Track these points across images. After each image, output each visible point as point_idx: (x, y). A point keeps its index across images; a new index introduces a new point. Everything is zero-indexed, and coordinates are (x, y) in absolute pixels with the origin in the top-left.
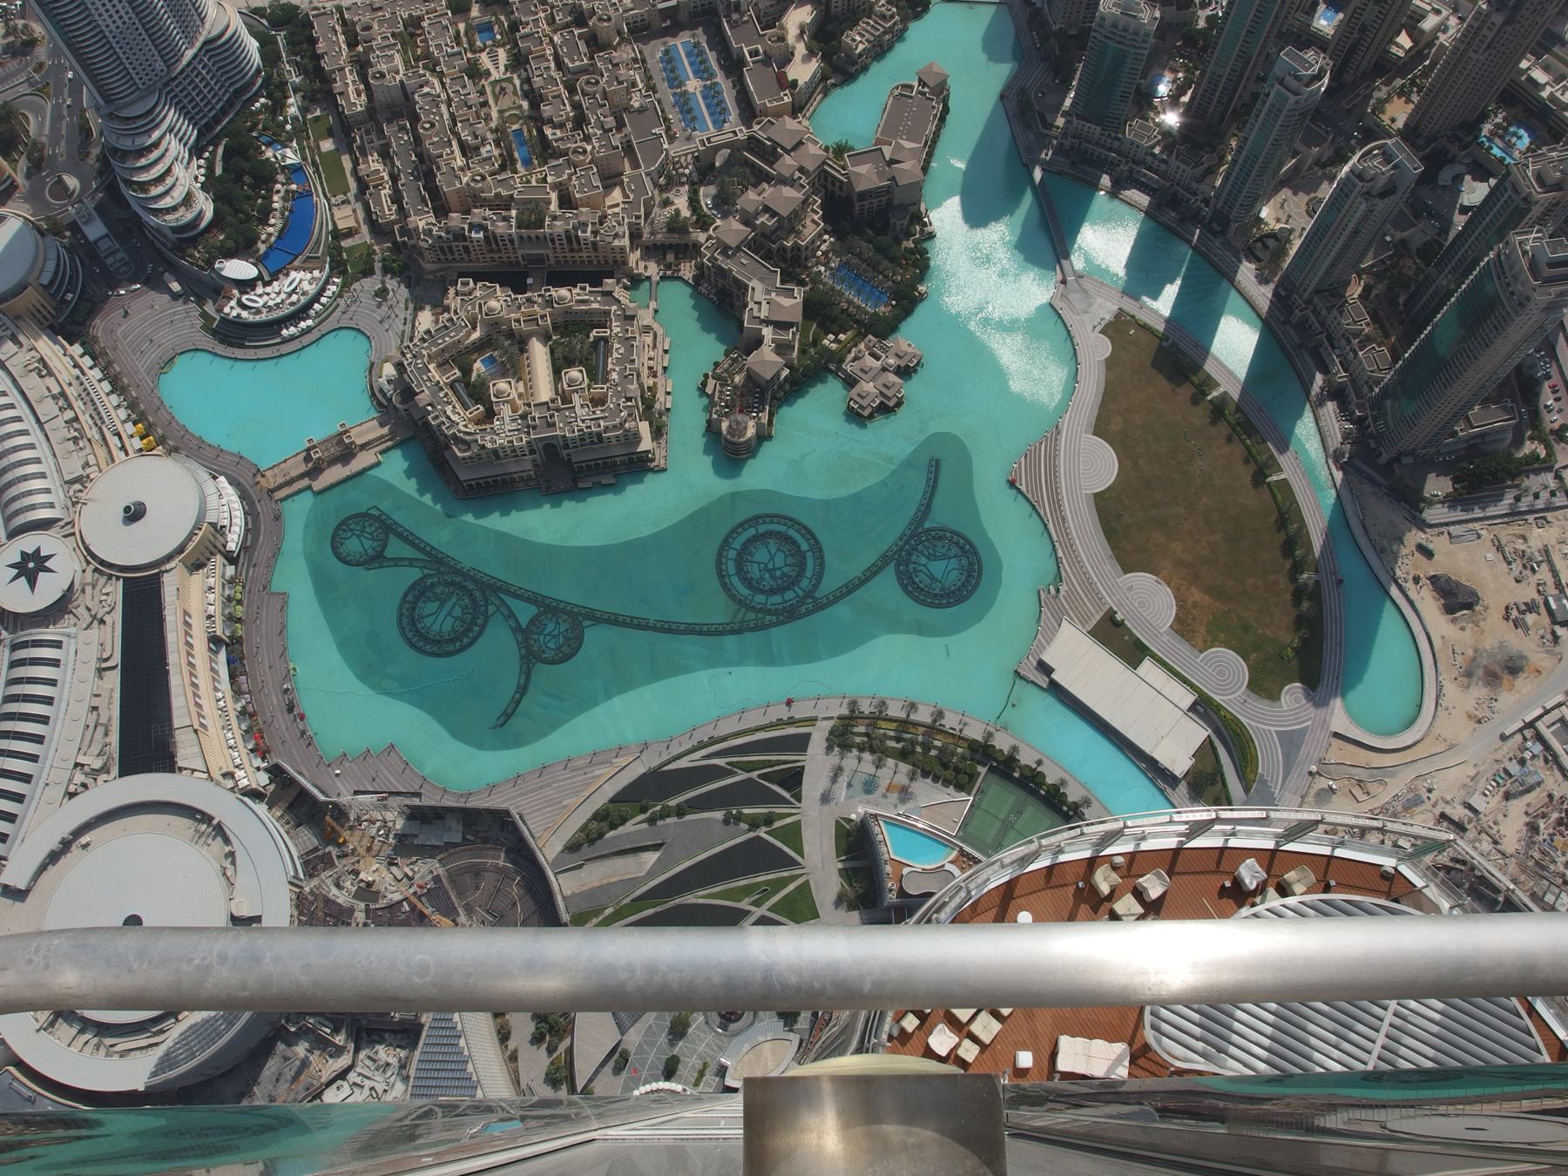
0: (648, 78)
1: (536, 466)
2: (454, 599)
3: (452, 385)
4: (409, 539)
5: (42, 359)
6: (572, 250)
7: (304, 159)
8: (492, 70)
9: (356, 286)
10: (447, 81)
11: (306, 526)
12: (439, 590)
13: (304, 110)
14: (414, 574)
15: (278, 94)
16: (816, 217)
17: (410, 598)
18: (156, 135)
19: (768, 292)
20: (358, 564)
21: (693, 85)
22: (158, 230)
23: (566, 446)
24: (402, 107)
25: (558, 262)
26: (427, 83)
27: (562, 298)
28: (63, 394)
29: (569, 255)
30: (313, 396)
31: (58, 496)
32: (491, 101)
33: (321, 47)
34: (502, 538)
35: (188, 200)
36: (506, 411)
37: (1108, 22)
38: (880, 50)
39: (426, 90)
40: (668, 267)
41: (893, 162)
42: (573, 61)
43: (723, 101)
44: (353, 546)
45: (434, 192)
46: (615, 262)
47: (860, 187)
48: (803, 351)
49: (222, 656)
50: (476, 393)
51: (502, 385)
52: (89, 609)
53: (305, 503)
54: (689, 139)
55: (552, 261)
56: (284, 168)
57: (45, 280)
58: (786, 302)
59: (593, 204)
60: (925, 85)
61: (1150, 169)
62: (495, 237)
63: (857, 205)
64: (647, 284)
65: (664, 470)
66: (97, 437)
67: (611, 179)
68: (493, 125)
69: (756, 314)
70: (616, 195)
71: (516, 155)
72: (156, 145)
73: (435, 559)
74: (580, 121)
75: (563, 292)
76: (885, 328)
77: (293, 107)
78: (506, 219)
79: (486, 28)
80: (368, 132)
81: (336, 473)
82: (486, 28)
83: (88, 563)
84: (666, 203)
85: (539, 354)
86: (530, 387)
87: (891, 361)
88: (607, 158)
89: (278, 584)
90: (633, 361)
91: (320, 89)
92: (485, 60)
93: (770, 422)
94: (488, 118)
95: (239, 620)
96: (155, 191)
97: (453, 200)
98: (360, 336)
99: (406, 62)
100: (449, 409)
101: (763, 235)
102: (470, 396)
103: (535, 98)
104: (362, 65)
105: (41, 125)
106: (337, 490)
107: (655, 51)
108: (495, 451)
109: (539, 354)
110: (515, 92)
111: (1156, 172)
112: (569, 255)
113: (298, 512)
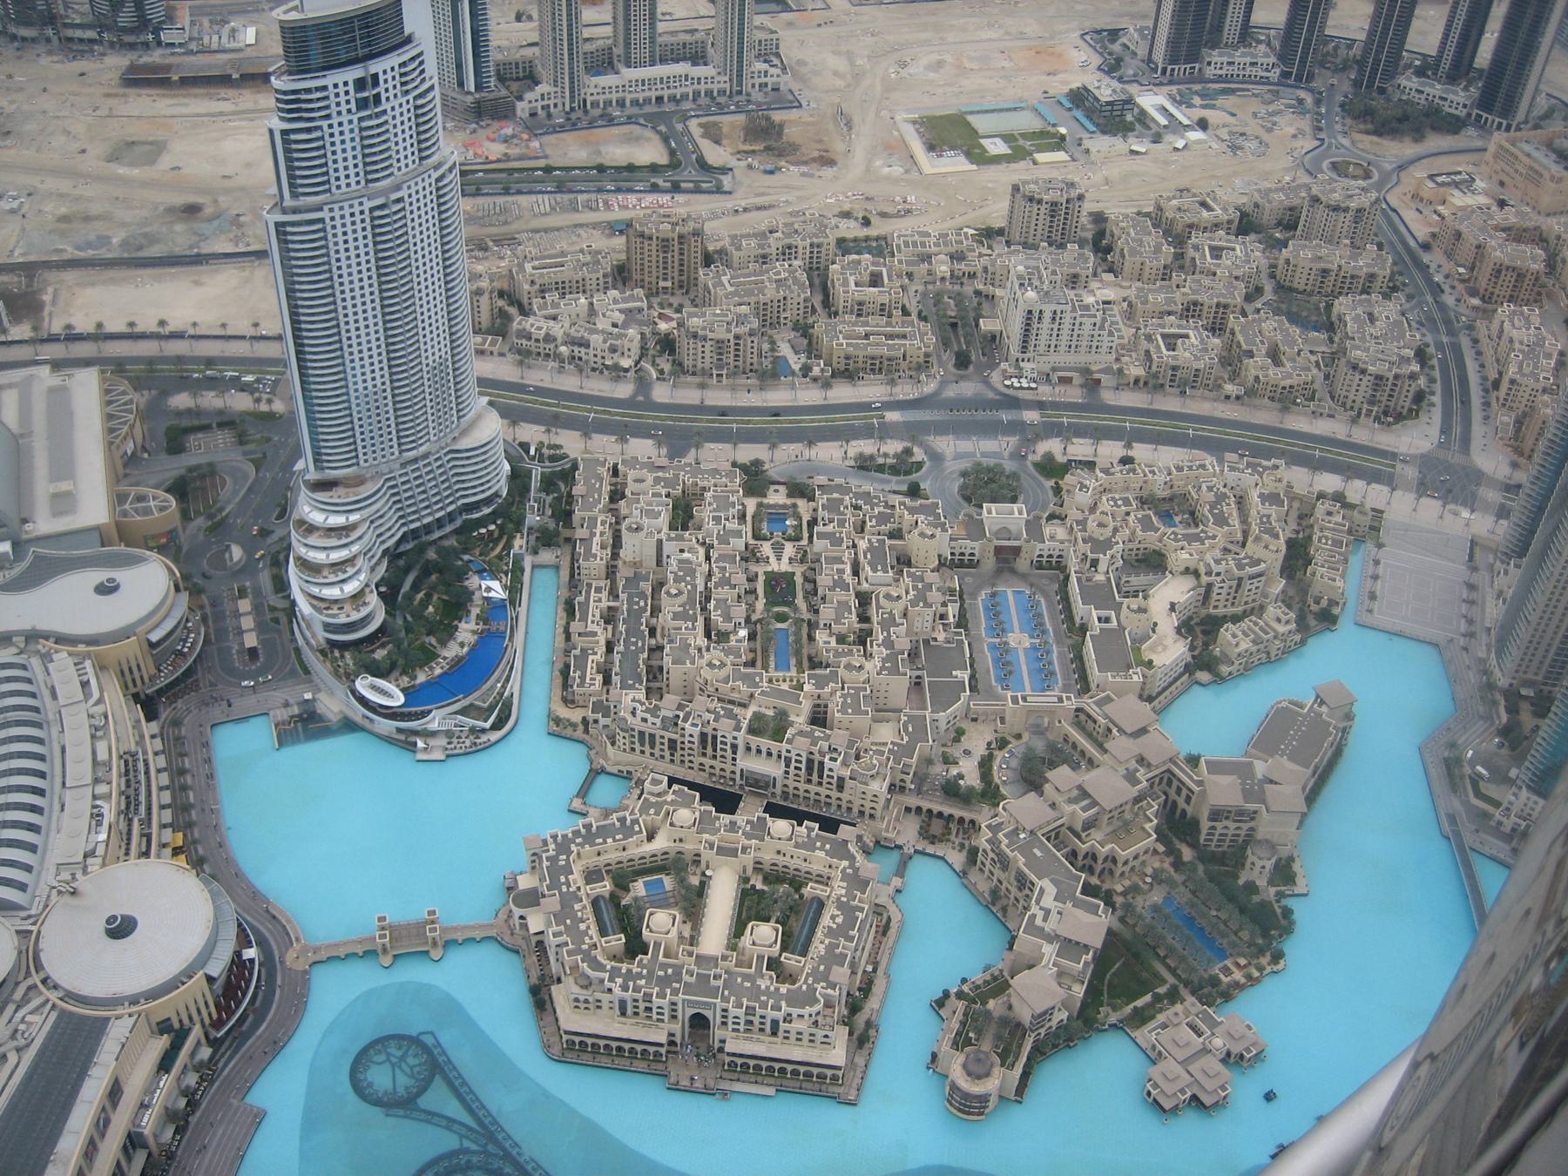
1: (672, 1043)
3: (595, 903)
4: (460, 1090)
6: (809, 781)
8: (772, 559)
10: (714, 555)
14: (448, 1142)
16: (1148, 826)
18: (354, 518)
20: (377, 1103)
21: (1019, 640)
25: (785, 795)
29: (803, 786)
33: (578, 490)
34: (592, 1134)
35: (357, 597)
38: (1268, 657)
39: (686, 555)
40: (933, 840)
42: (875, 570)
43: (1050, 663)
44: (380, 1077)
45: (655, 673)
46: (862, 813)
55: (778, 790)
57: (155, 637)
60: (1322, 703)
62: (715, 737)
63: (1205, 825)
64: (895, 857)
65: (852, 1104)
68: (754, 618)
73: (487, 1130)
75: (781, 826)
80: (598, 590)
82: (777, 516)
87: (1218, 1042)
92: (766, 548)
94: (751, 608)
101: (1070, 829)
105: (235, 493)
112: (803, 786)
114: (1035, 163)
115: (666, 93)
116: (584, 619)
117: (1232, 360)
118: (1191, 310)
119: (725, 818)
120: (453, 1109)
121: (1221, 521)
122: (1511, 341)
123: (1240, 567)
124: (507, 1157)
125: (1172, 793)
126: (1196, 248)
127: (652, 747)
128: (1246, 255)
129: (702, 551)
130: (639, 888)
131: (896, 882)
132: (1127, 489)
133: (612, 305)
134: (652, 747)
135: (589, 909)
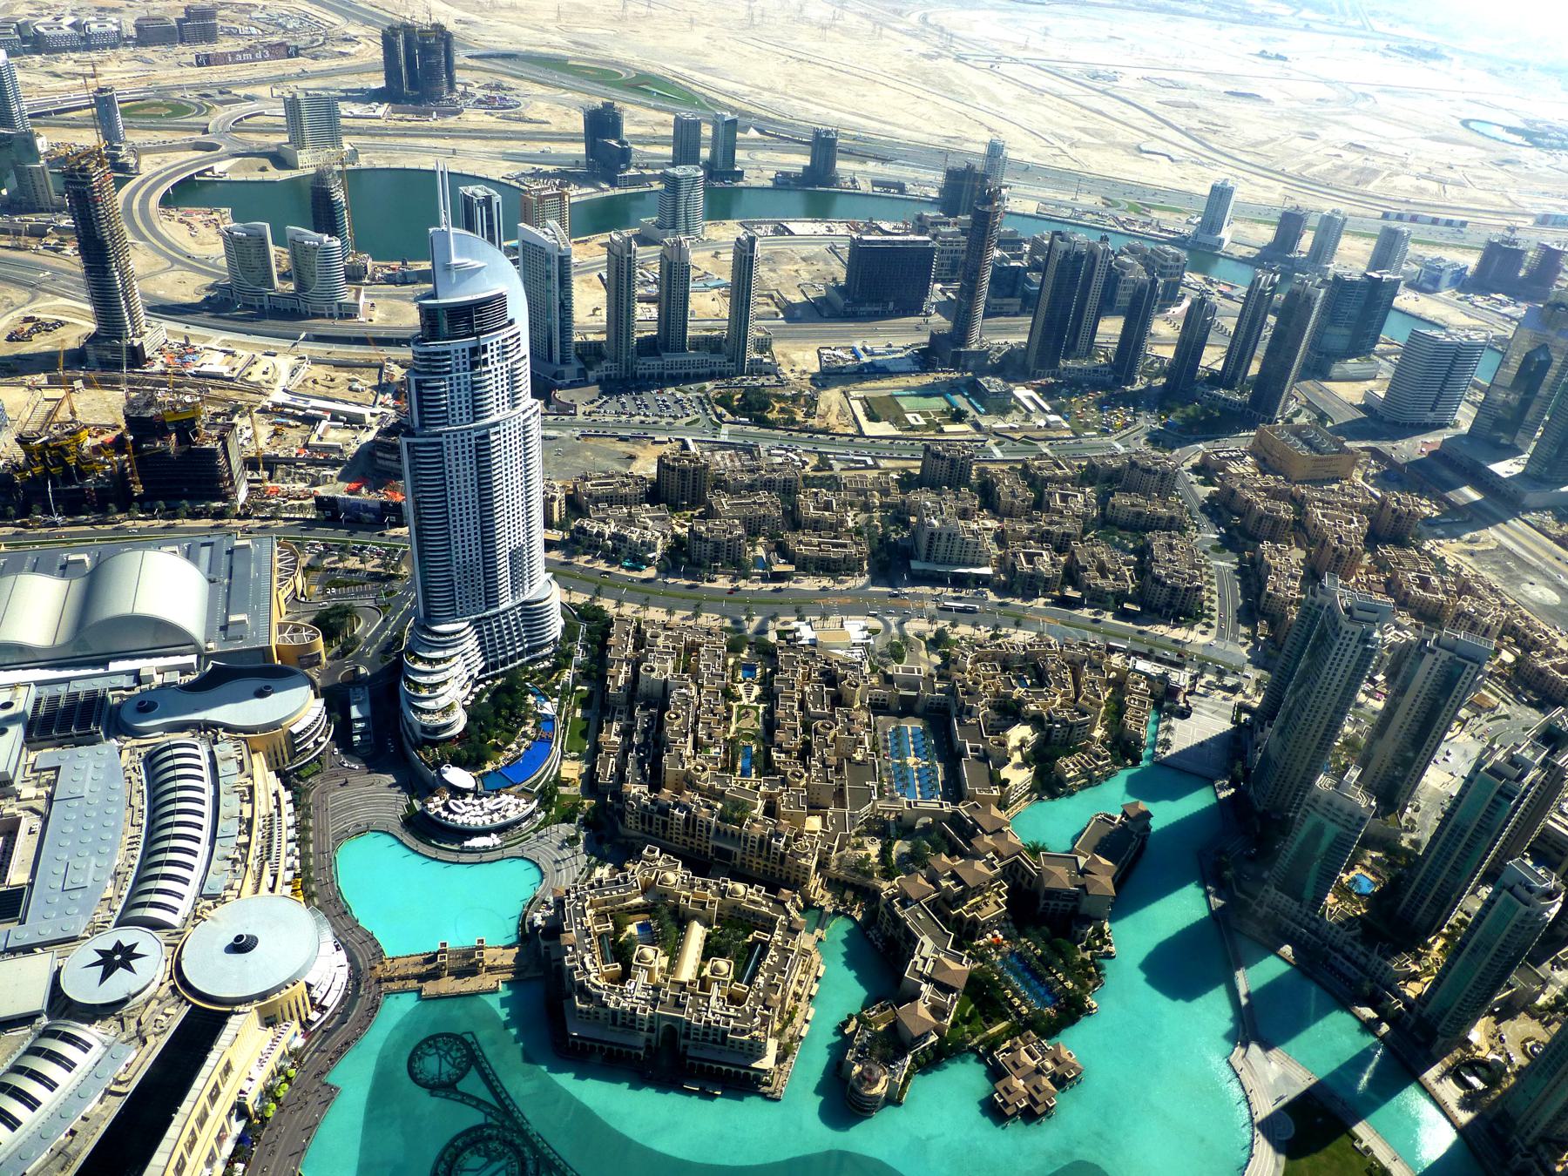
0: (874, 744)
1: (648, 1047)
2: (503, 1162)
4: (489, 1079)
5: (251, 788)
7: (559, 714)
9: (554, 828)
10: (704, 692)
11: (397, 1028)
12: (492, 1145)
13: (576, 682)
14: (474, 1117)
15: (562, 660)
17: (459, 1143)
18: (449, 652)
19: (936, 951)
20: (425, 1085)
22: (410, 725)
23: (687, 1036)
24: (659, 700)
25: (743, 865)
26: (687, 687)
27: (734, 891)
28: (250, 822)
30: (465, 907)
31: (185, 907)
32: (734, 719)
33: (612, 640)
34: (585, 1115)
36: (642, 977)
37: (1324, 798)
40: (843, 902)
41: (1083, 872)
44: (431, 1065)
46: (796, 881)
47: (1050, 884)
48: (954, 1024)
49: (237, 1127)
50: (620, 953)
51: (649, 951)
52: (139, 1023)
53: (408, 1002)
54: (893, 799)
55: (738, 862)
56: (536, 714)
57: (295, 730)
58: (953, 966)
59: (790, 817)
61: (1348, 958)
63: (1042, 902)
65: (778, 1100)
66: (256, 868)
67: (815, 808)
69: (919, 968)
70: (814, 823)
71: (740, 764)
72: (445, 660)
73: (503, 1109)
74: (805, 752)
75: (740, 887)
76: (1050, 1030)
77: (567, 675)
78: (709, 807)
79: (750, 669)
80: (620, 712)
81: (447, 985)
83: (171, 977)
84: (860, 846)
85: (697, 934)
86: (673, 967)
87: (1049, 1064)
88: (820, 788)
89: (332, 1078)
90: (783, 973)
91: (596, 671)
93: (904, 1085)
94: (727, 729)
95: (276, 1100)
96: (425, 693)
97: (669, 778)
98: (535, 873)
99: (675, 670)
100: (586, 960)
101: (945, 900)
102: (612, 952)
103: (771, 724)
104: (636, 665)
106: (443, 1003)
107: (888, 724)
108: (614, 1012)
109: (697, 934)
110: (757, 719)
111: (1355, 963)
113: (398, 1009)
114: (941, 431)
115: (692, 371)
116: (609, 732)
117: (1072, 575)
118: (1044, 538)
119: (698, 880)
120: (483, 1093)
121: (1061, 683)
122: (1269, 567)
123: (1073, 717)
124: (522, 1133)
125: (1019, 879)
126: (1050, 494)
127: (650, 825)
128: (1082, 500)
129: (694, 688)
130: (632, 929)
131: (818, 932)
132: (994, 659)
133: (645, 513)
134: (650, 825)
135: (596, 943)
